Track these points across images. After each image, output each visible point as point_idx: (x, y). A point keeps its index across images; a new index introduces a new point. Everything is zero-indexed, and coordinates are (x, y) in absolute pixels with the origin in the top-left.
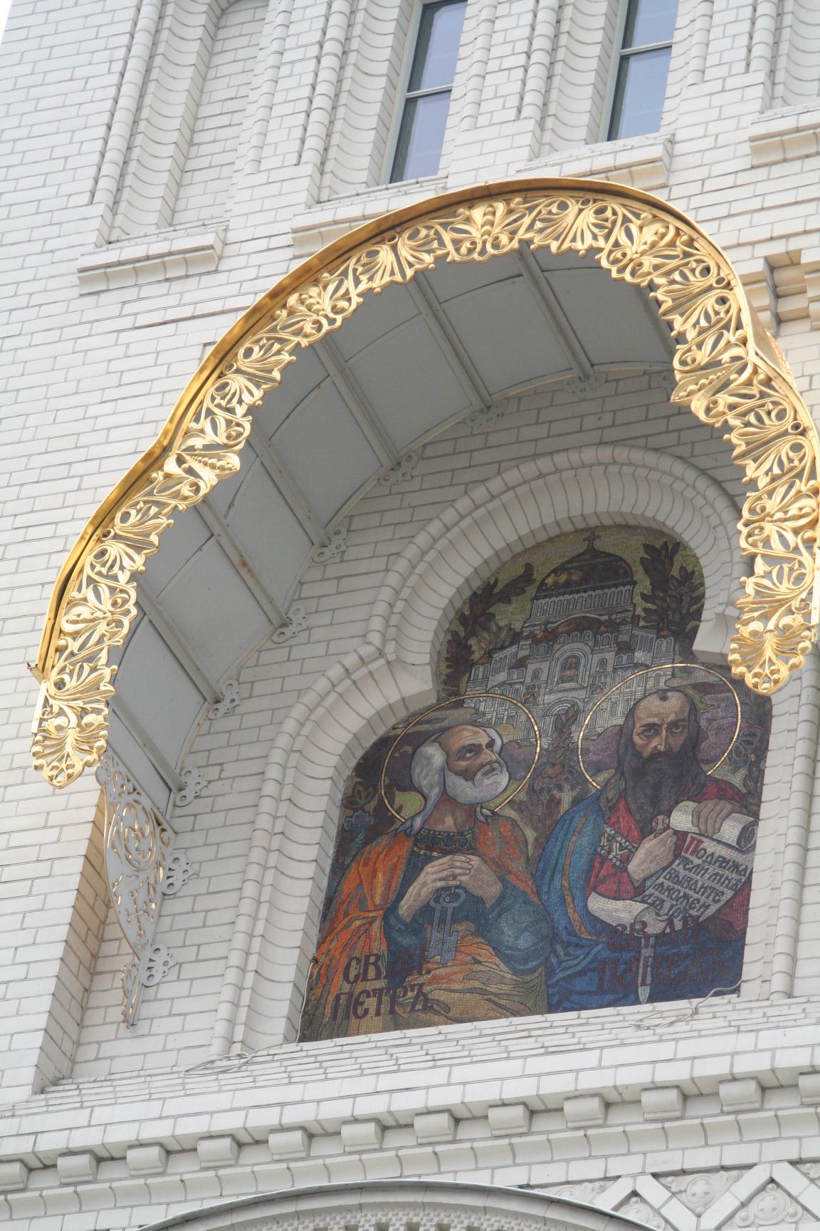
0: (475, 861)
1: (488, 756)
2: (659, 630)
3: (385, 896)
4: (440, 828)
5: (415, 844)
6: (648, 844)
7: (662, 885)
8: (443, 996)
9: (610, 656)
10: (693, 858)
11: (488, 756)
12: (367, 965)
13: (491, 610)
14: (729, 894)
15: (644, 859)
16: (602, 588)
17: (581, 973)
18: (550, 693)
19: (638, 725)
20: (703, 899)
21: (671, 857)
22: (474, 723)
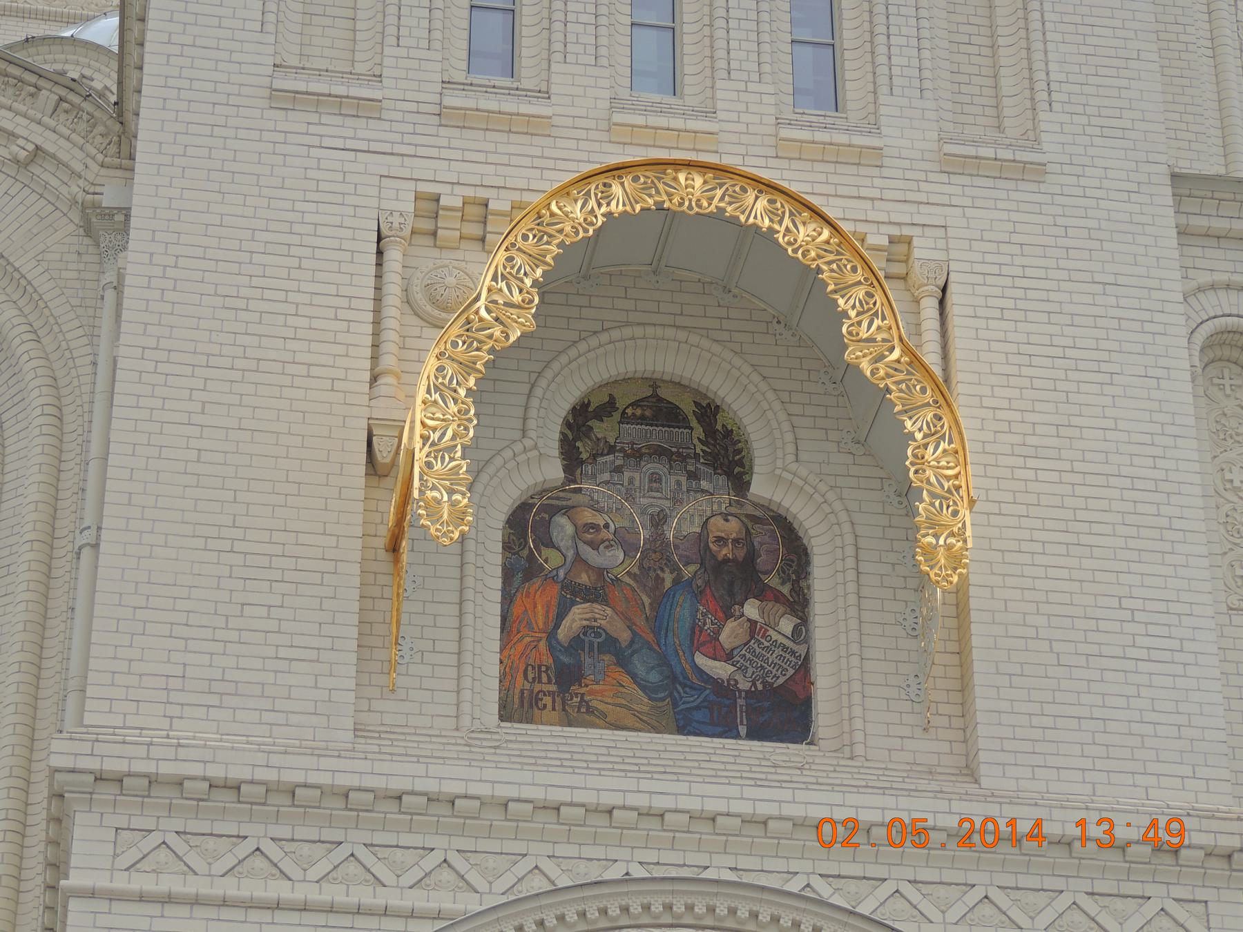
0: (609, 611)
1: (605, 534)
2: (715, 469)
4: (578, 581)
5: (562, 588)
6: (731, 625)
8: (601, 706)
9: (683, 479)
11: (605, 534)
15: (730, 634)
16: (669, 426)
17: (698, 708)
18: (644, 497)
22: (592, 507)
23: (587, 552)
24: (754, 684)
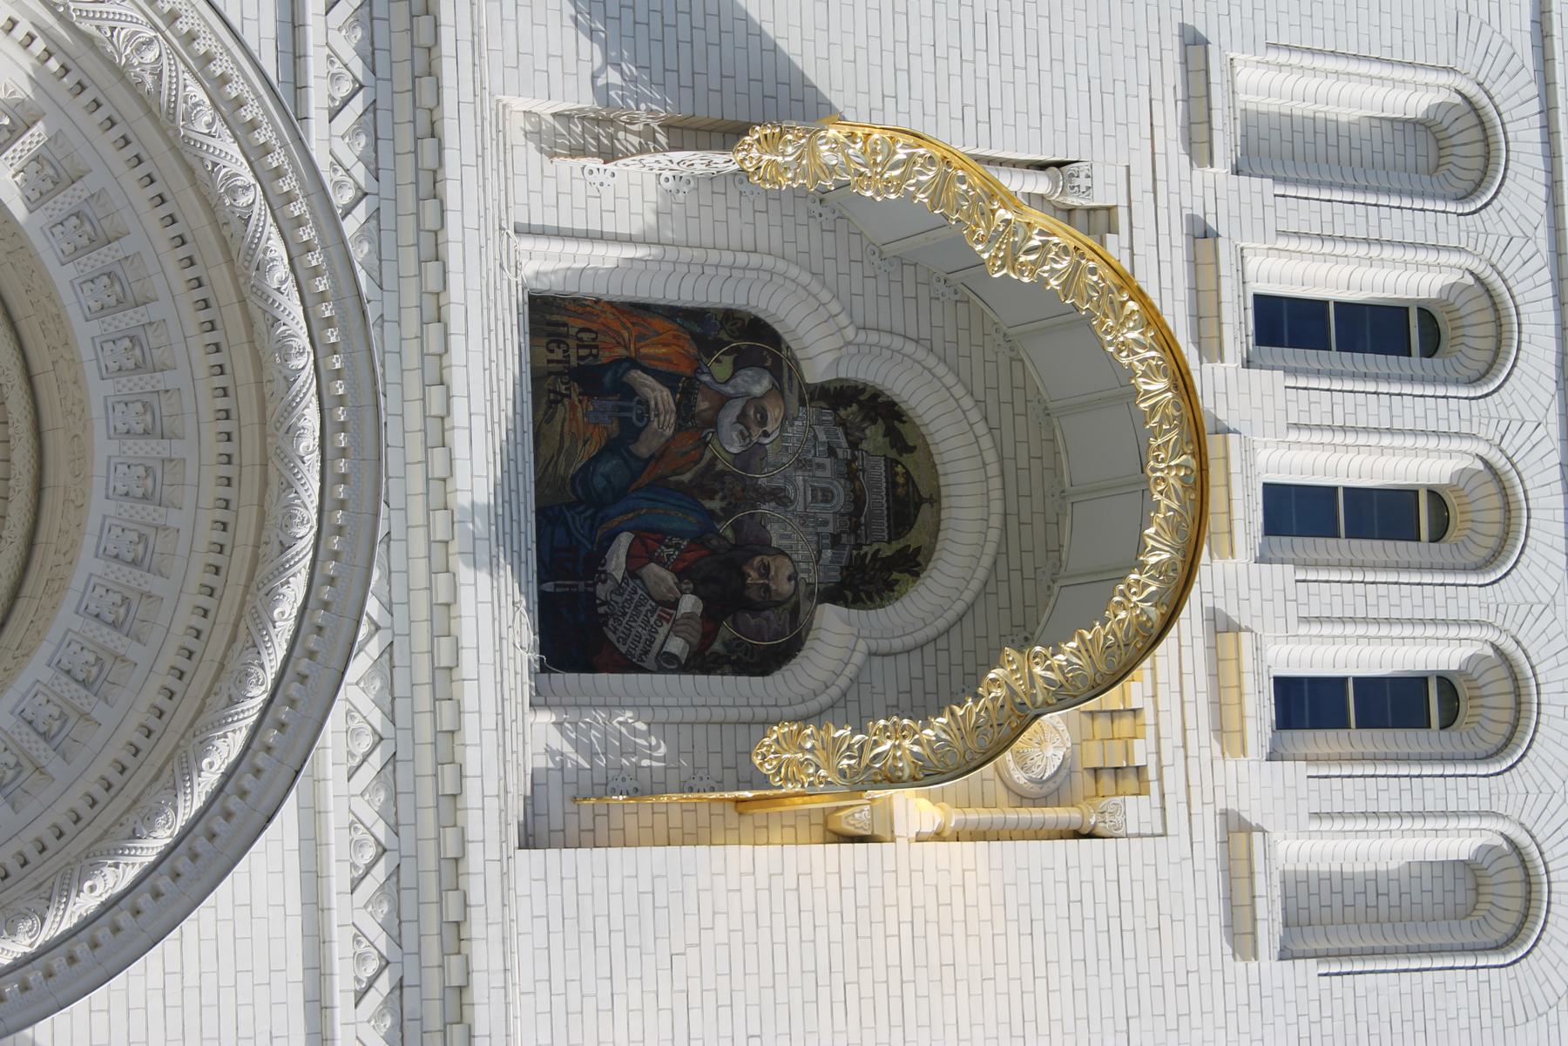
0: (669, 432)
2: (847, 568)
3: (646, 357)
4: (700, 398)
6: (670, 578)
9: (830, 529)
11: (756, 433)
12: (591, 347)
13: (880, 421)
14: (623, 649)
15: (659, 576)
21: (657, 598)
22: (785, 418)
24: (604, 603)
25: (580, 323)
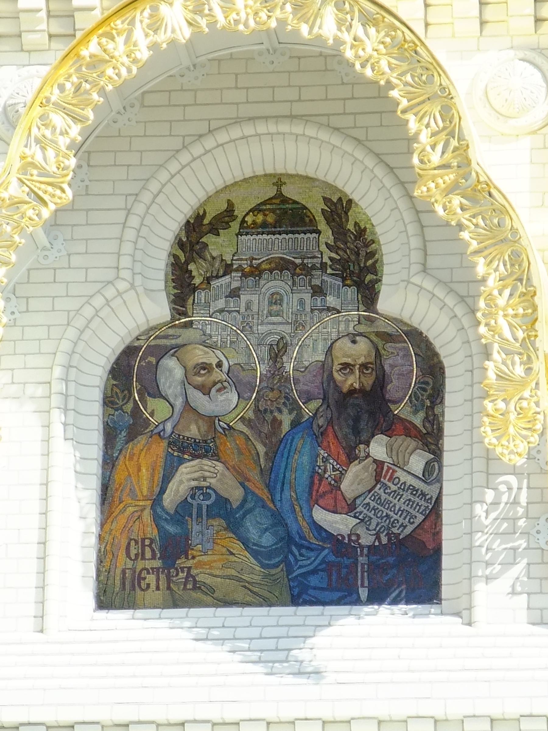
0: (220, 466)
2: (344, 279)
3: (151, 489)
4: (187, 434)
5: (169, 444)
6: (354, 469)
7: (368, 504)
8: (209, 580)
9: (307, 297)
10: (390, 484)
11: (219, 375)
12: (143, 546)
13: (204, 240)
14: (420, 518)
15: (354, 480)
16: (293, 233)
17: (314, 572)
18: (262, 324)
19: (336, 363)
20: (401, 520)
22: (203, 344)
23: (198, 399)
24: (378, 538)
25: (122, 554)
